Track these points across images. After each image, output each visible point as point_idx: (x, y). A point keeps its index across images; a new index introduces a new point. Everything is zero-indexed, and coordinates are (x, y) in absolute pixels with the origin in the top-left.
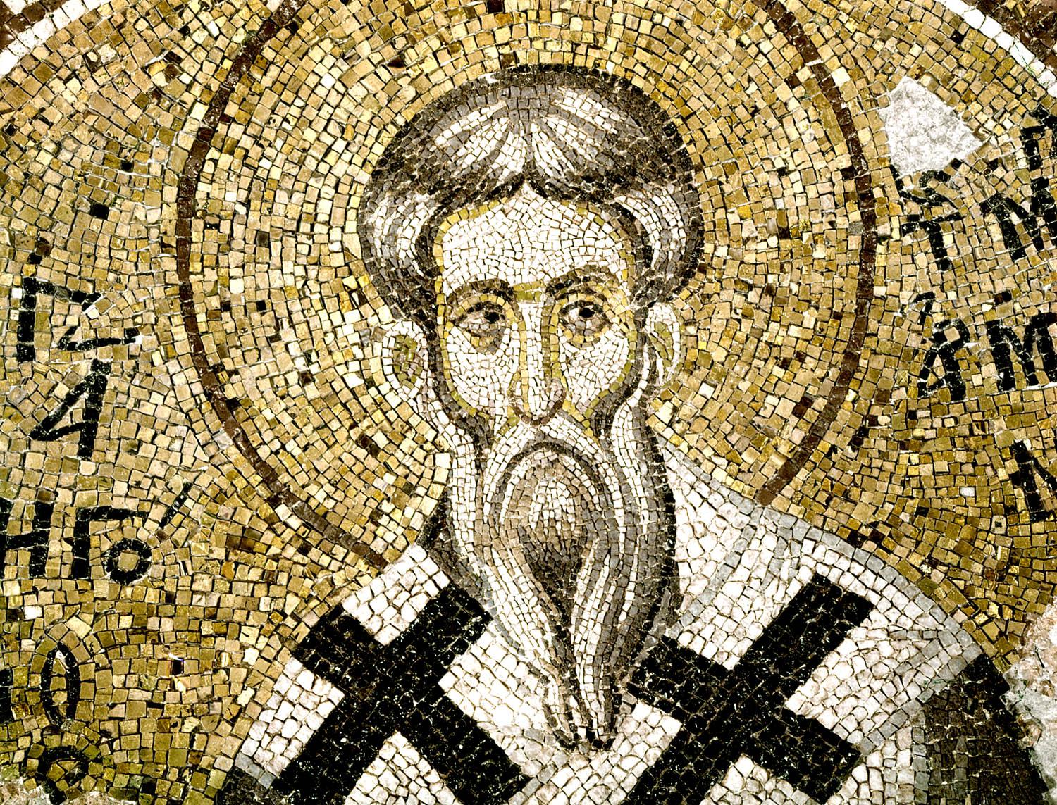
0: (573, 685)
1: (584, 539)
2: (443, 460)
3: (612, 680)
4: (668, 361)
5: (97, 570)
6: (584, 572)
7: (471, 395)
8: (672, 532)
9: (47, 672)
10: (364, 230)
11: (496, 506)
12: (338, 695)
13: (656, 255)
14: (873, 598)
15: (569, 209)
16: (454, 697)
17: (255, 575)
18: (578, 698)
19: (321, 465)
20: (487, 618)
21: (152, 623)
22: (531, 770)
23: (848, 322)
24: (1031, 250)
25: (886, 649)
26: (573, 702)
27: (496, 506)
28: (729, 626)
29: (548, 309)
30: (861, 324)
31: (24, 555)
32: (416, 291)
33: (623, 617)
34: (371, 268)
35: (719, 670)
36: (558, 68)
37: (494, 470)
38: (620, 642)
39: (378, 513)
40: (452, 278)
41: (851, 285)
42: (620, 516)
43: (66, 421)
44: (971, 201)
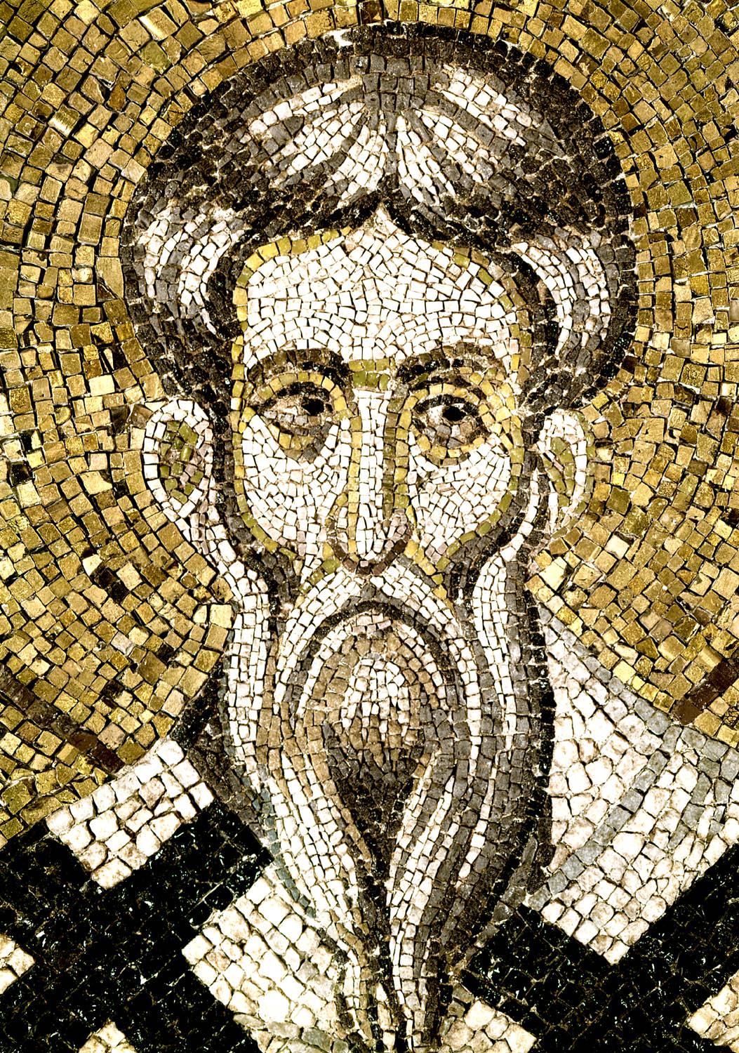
0: (382, 968)
1: (419, 749)
2: (221, 615)
4: (565, 498)
6: (414, 800)
7: (272, 522)
8: (548, 748)
10: (132, 254)
11: (294, 690)
13: (563, 337)
15: (443, 255)
16: (204, 973)
18: (389, 987)
19: (34, 608)
20: (266, 858)
26: (380, 994)
27: (294, 690)
28: (618, 899)
29: (396, 402)
33: (465, 872)
35: (598, 961)
36: (446, 33)
37: (296, 636)
38: (458, 909)
39: (114, 688)
40: (255, 345)
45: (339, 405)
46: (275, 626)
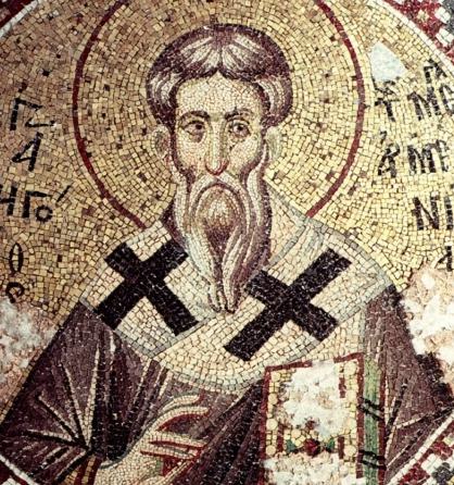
0: (221, 287)
2: (173, 186)
3: (238, 287)
4: (274, 152)
5: (32, 216)
6: (230, 240)
9: (12, 253)
10: (148, 87)
11: (194, 209)
12: (122, 279)
13: (272, 106)
14: (351, 259)
15: (236, 83)
16: (169, 286)
17: (92, 225)
18: (223, 293)
19: (122, 184)
20: (186, 255)
21: (51, 240)
22: (199, 318)
23: (351, 141)
24: (426, 116)
25: (354, 281)
26: (220, 293)
27: (194, 209)
28: (291, 268)
30: (356, 142)
33: (245, 260)
34: (150, 102)
38: (243, 271)
41: (353, 126)
42: (248, 218)
43: (24, 156)
44: (403, 94)
45: (206, 126)
46: (189, 191)
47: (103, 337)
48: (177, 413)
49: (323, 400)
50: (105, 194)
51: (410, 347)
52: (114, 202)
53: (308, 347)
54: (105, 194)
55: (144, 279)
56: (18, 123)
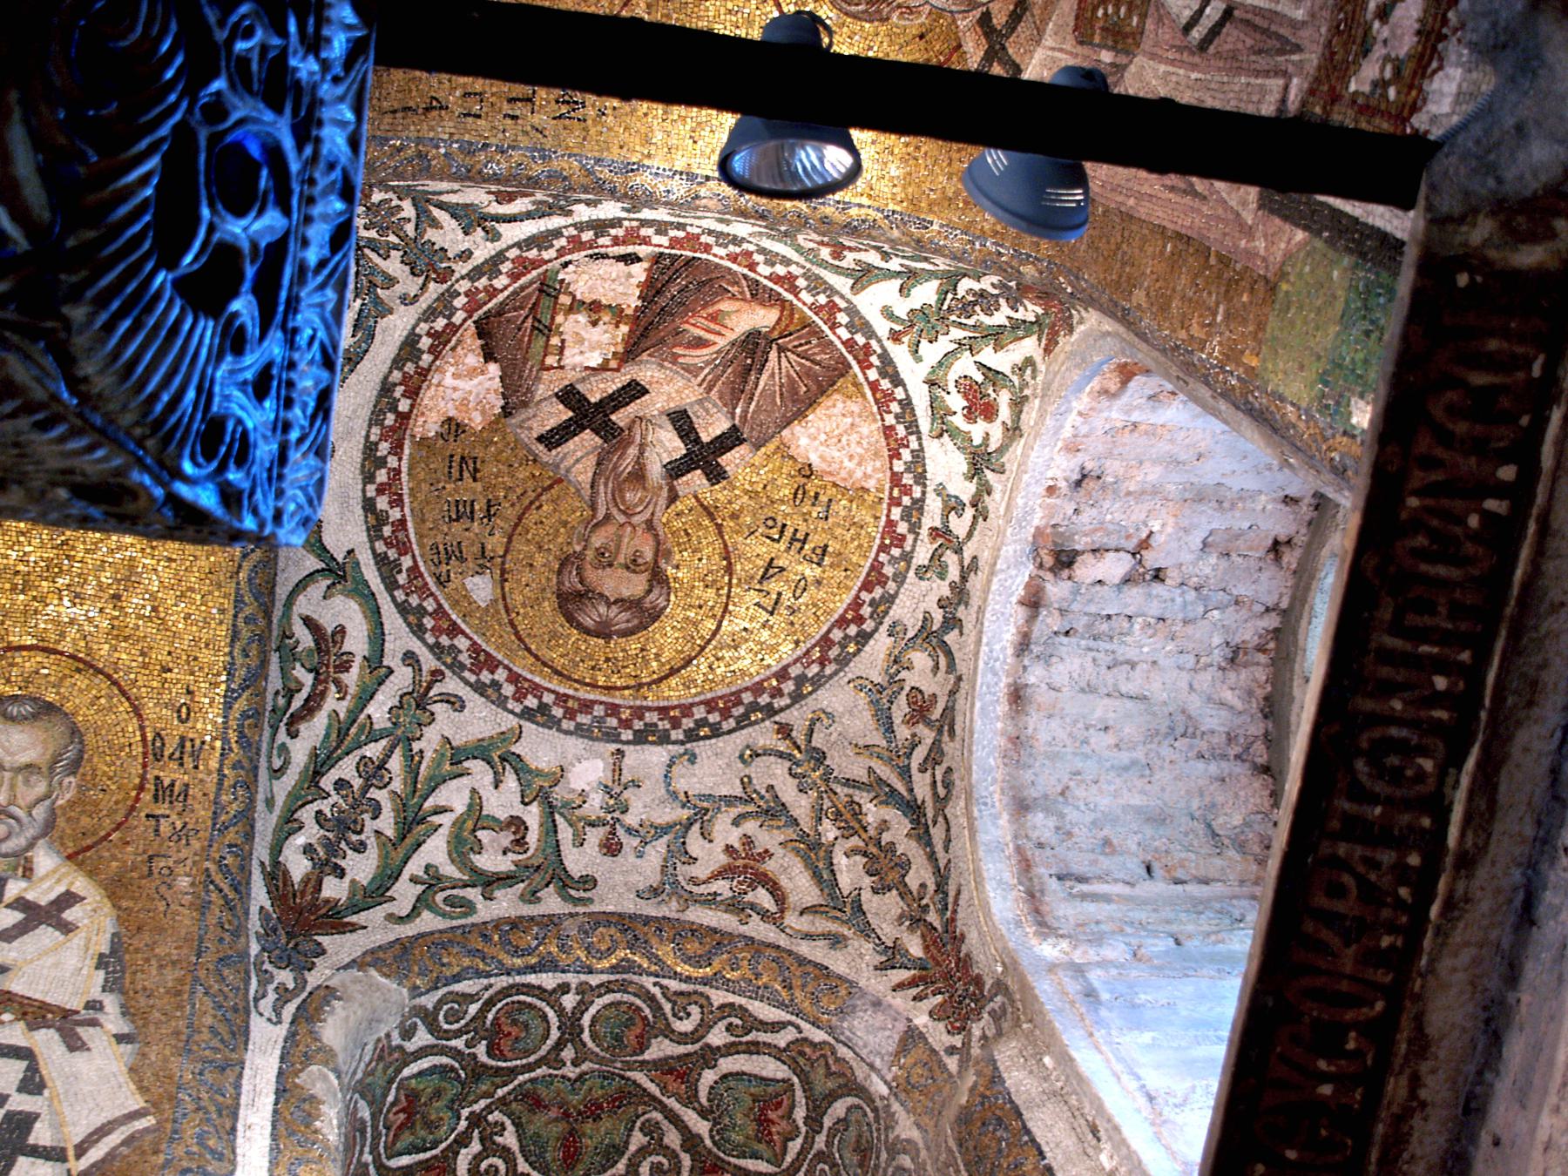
31: (798, 536)
32: (658, 578)
47: (744, 417)
48: (698, 352)
49: (580, 341)
50: (719, 527)
51: (502, 369)
52: (713, 519)
53: (583, 380)
54: (719, 527)
55: (703, 457)
56: (774, 596)
